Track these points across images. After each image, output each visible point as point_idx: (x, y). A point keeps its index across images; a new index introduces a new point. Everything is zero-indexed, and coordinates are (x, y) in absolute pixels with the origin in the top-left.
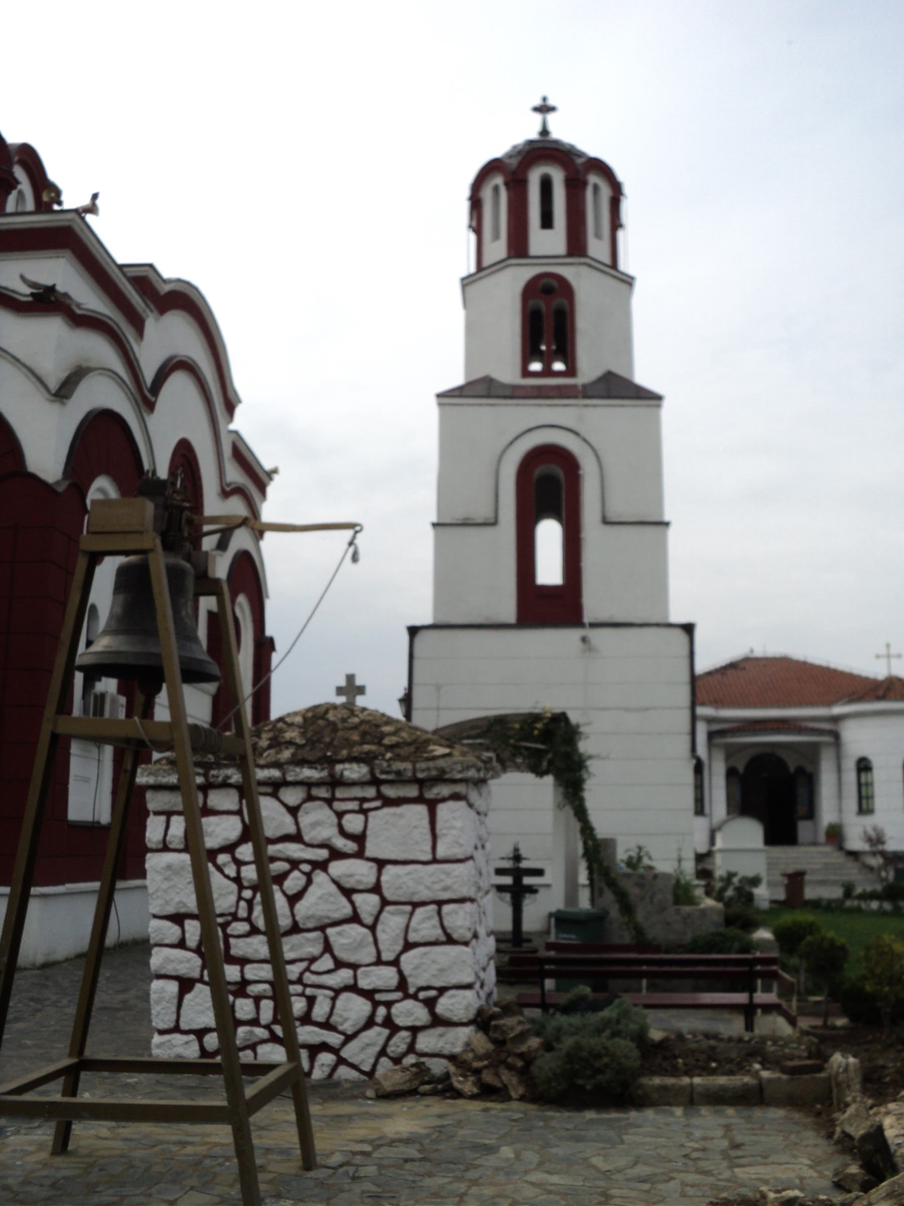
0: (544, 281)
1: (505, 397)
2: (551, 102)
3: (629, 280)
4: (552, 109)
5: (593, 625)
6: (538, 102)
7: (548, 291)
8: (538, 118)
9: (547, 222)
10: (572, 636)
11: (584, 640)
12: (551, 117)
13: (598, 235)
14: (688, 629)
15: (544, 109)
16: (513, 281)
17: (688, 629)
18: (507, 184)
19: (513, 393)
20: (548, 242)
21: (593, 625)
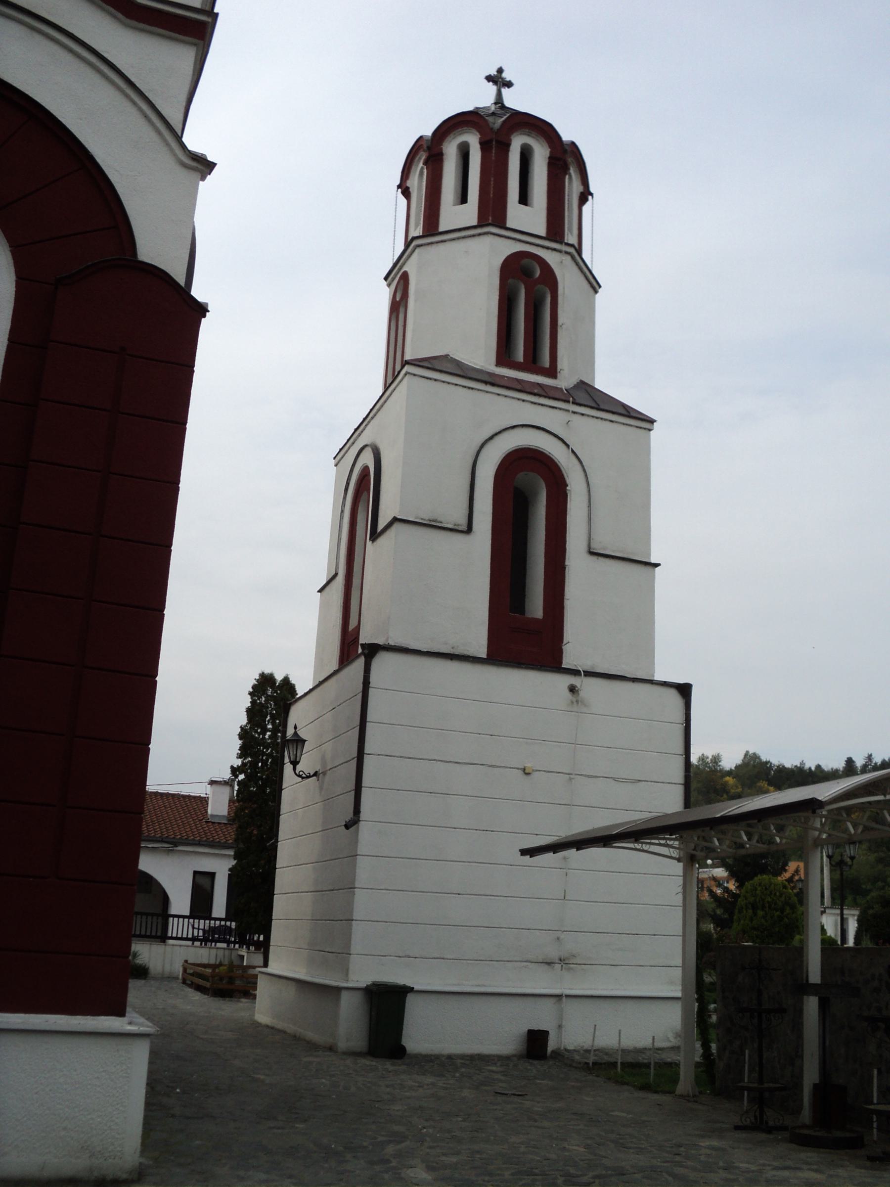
0: (526, 261)
1: (486, 383)
2: (507, 76)
3: (597, 287)
4: (509, 84)
5: (589, 674)
6: (493, 72)
7: (526, 273)
8: (492, 89)
9: (524, 199)
10: (563, 681)
11: (572, 689)
12: (505, 91)
13: (570, 230)
14: (685, 690)
15: (498, 80)
16: (491, 251)
17: (685, 690)
18: (485, 146)
19: (491, 381)
20: (528, 218)
21: (589, 674)
